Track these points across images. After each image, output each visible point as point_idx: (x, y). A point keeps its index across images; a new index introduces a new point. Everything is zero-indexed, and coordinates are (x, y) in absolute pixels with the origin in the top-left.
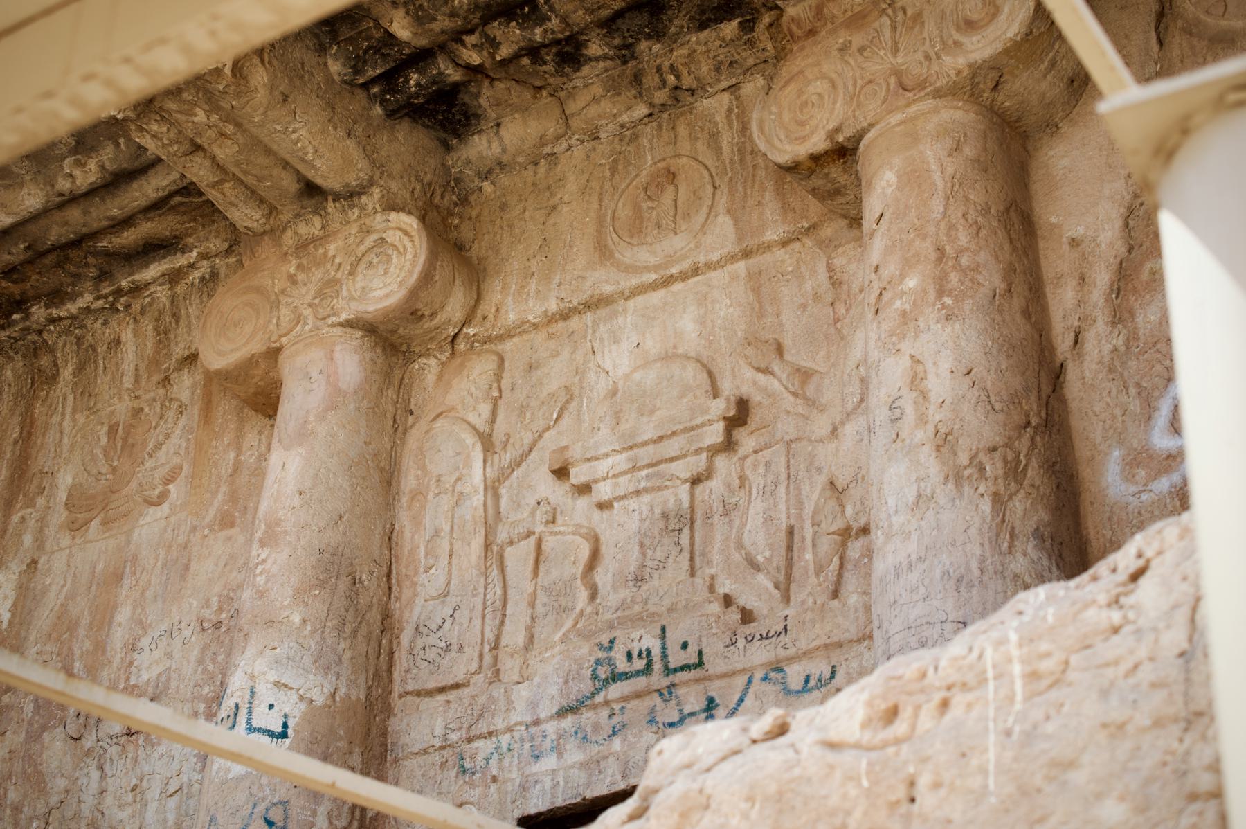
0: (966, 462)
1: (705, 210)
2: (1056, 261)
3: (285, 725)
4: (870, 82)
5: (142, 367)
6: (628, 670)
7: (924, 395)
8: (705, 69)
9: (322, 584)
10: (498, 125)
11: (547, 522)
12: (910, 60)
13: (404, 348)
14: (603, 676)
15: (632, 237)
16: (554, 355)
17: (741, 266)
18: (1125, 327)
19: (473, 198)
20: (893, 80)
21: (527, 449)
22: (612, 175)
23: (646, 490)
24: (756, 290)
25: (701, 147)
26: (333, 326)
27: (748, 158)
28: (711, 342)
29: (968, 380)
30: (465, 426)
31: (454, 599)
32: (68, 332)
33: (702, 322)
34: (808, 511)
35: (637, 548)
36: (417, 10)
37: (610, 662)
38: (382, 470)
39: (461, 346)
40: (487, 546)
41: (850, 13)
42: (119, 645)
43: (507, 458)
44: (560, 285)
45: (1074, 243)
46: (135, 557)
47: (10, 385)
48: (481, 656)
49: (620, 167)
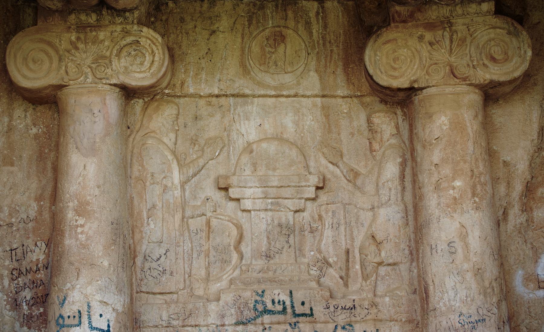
0: (488, 286)
3: (109, 326)
4: (436, 64)
6: (273, 309)
7: (466, 246)
11: (214, 211)
12: (460, 62)
13: (132, 94)
14: (260, 310)
15: (260, 65)
16: (211, 115)
17: (319, 100)
18: (527, 214)
19: (163, 8)
20: (448, 68)
21: (201, 168)
23: (271, 210)
24: (327, 116)
25: (301, 27)
26: (105, 84)
27: (328, 45)
31: (166, 245)
33: (296, 123)
34: (357, 244)
35: (265, 239)
37: (263, 303)
41: (426, 21)
44: (220, 80)
48: (185, 281)
49: (254, 22)
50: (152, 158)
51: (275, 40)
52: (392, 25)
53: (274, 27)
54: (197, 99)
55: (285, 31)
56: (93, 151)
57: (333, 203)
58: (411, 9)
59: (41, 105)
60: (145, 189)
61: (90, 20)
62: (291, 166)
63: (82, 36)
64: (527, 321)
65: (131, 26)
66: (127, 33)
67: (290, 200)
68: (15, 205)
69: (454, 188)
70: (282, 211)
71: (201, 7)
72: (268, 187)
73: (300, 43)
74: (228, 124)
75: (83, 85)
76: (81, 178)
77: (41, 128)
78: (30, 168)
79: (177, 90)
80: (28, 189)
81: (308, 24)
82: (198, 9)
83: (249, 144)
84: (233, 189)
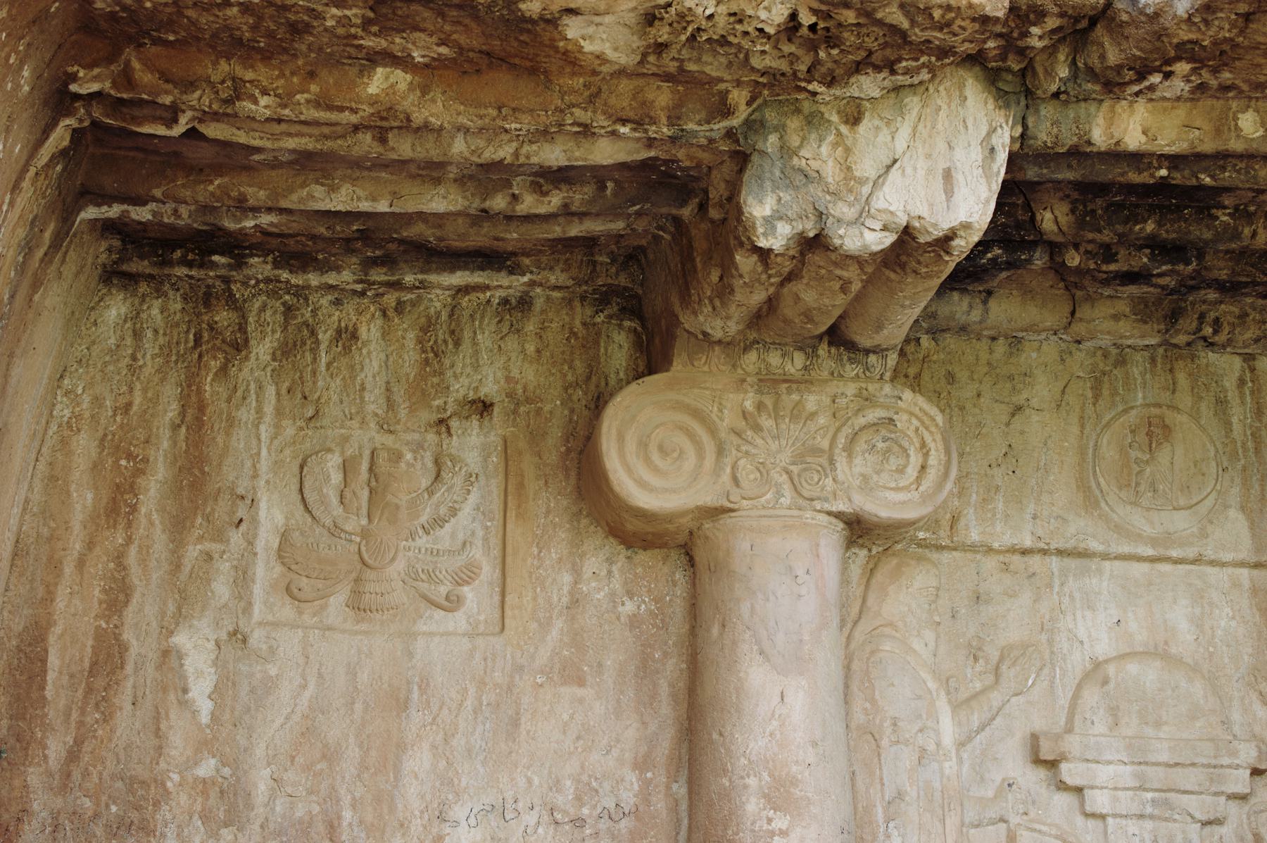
10: (989, 293)
15: (1120, 488)
16: (1011, 595)
17: (1245, 572)
22: (1096, 397)
23: (1151, 817)
25: (1206, 409)
26: (819, 511)
28: (1211, 654)
36: (1086, 213)
42: (416, 805)
43: (975, 721)
46: (424, 686)
47: (156, 331)
49: (1106, 392)
50: (893, 685)
51: (1149, 434)
53: (1148, 405)
54: (978, 557)
55: (1170, 417)
59: (645, 550)
60: (879, 755)
61: (789, 368)
63: (769, 401)
65: (877, 386)
66: (867, 400)
67: (1193, 797)
68: (590, 776)
70: (1175, 821)
71: (991, 351)
72: (1146, 763)
73: (1204, 445)
74: (1047, 617)
75: (772, 512)
76: (775, 723)
77: (644, 602)
78: (622, 692)
79: (942, 533)
80: (618, 741)
81: (1221, 403)
82: (984, 356)
83: (1097, 665)
84: (1071, 766)
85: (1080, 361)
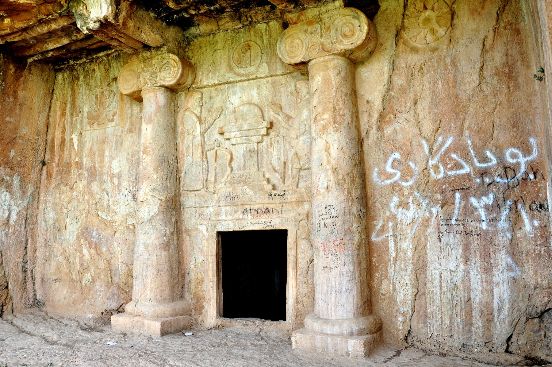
1: (259, 61)
2: (363, 107)
5: (102, 79)
7: (329, 153)
8: (260, 18)
9: (161, 166)
10: (199, 25)
12: (326, 41)
16: (217, 96)
17: (270, 78)
19: (191, 43)
20: (321, 46)
24: (274, 87)
25: (258, 40)
27: (272, 46)
29: (342, 152)
30: (194, 115)
32: (80, 66)
33: (259, 94)
38: (172, 128)
39: (191, 89)
40: (202, 152)
42: (107, 162)
43: (206, 126)
45: (368, 102)
46: (108, 137)
48: (203, 184)
52: (290, 26)
56: (150, 121)
57: (278, 136)
58: (297, 14)
62: (254, 118)
64: (380, 199)
69: (323, 119)
85: (229, 34)
